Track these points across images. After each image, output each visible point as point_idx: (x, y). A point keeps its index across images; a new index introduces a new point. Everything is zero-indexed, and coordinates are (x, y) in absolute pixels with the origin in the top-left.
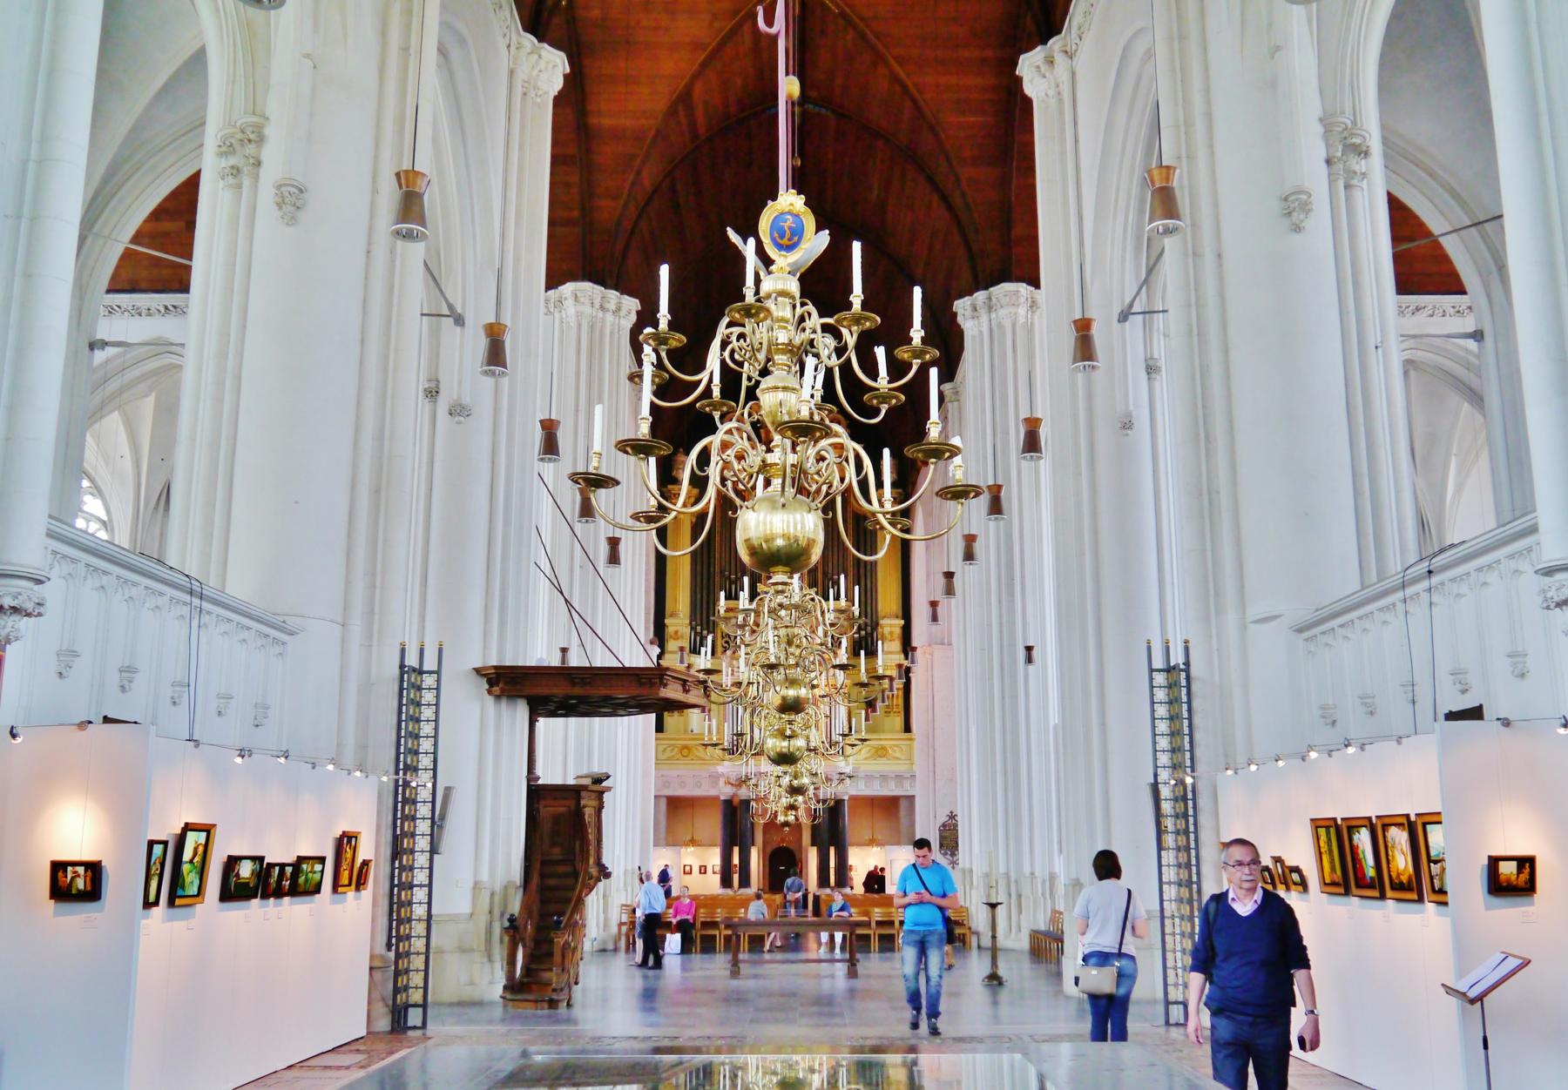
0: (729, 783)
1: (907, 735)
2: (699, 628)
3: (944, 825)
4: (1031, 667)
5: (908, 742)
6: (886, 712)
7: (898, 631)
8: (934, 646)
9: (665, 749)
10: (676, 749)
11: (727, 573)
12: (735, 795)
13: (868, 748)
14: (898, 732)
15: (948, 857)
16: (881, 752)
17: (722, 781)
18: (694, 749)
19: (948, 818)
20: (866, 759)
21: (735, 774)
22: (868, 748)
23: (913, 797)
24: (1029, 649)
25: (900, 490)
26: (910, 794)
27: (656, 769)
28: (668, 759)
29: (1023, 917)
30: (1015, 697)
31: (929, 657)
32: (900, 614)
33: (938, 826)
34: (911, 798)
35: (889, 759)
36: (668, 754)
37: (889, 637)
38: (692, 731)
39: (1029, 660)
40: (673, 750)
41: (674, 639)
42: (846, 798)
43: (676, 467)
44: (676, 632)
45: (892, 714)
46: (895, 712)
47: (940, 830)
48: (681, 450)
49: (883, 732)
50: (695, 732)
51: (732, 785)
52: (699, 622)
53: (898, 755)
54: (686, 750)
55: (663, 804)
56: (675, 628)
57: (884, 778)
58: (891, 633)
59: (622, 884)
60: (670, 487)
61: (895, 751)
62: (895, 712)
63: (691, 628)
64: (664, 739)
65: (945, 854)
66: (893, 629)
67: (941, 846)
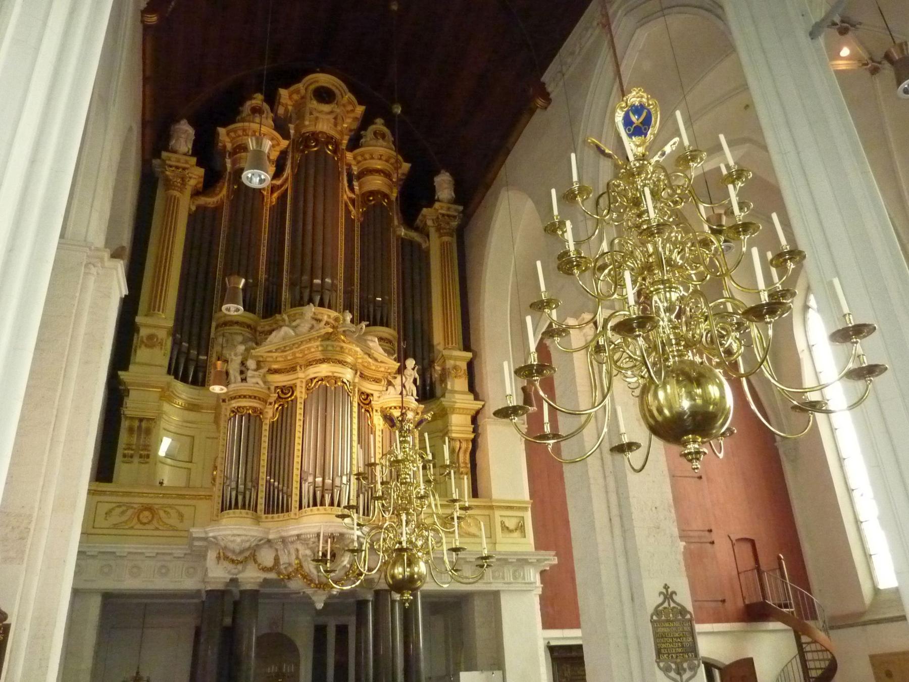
0: (226, 558)
3: (657, 612)
5: (486, 512)
7: (464, 365)
9: (113, 509)
10: (130, 512)
12: (234, 581)
15: (673, 674)
17: (211, 555)
18: (162, 513)
19: (662, 597)
21: (238, 540)
23: (496, 595)
25: (461, 208)
26: (493, 587)
27: (91, 492)
28: (115, 526)
36: (114, 519)
38: (161, 483)
40: (123, 513)
41: (146, 346)
44: (151, 337)
47: (652, 622)
50: (166, 483)
51: (233, 561)
54: (146, 513)
55: (95, 605)
60: (164, 154)
61: (469, 525)
64: (112, 493)
65: (666, 670)
66: (458, 363)
67: (659, 652)
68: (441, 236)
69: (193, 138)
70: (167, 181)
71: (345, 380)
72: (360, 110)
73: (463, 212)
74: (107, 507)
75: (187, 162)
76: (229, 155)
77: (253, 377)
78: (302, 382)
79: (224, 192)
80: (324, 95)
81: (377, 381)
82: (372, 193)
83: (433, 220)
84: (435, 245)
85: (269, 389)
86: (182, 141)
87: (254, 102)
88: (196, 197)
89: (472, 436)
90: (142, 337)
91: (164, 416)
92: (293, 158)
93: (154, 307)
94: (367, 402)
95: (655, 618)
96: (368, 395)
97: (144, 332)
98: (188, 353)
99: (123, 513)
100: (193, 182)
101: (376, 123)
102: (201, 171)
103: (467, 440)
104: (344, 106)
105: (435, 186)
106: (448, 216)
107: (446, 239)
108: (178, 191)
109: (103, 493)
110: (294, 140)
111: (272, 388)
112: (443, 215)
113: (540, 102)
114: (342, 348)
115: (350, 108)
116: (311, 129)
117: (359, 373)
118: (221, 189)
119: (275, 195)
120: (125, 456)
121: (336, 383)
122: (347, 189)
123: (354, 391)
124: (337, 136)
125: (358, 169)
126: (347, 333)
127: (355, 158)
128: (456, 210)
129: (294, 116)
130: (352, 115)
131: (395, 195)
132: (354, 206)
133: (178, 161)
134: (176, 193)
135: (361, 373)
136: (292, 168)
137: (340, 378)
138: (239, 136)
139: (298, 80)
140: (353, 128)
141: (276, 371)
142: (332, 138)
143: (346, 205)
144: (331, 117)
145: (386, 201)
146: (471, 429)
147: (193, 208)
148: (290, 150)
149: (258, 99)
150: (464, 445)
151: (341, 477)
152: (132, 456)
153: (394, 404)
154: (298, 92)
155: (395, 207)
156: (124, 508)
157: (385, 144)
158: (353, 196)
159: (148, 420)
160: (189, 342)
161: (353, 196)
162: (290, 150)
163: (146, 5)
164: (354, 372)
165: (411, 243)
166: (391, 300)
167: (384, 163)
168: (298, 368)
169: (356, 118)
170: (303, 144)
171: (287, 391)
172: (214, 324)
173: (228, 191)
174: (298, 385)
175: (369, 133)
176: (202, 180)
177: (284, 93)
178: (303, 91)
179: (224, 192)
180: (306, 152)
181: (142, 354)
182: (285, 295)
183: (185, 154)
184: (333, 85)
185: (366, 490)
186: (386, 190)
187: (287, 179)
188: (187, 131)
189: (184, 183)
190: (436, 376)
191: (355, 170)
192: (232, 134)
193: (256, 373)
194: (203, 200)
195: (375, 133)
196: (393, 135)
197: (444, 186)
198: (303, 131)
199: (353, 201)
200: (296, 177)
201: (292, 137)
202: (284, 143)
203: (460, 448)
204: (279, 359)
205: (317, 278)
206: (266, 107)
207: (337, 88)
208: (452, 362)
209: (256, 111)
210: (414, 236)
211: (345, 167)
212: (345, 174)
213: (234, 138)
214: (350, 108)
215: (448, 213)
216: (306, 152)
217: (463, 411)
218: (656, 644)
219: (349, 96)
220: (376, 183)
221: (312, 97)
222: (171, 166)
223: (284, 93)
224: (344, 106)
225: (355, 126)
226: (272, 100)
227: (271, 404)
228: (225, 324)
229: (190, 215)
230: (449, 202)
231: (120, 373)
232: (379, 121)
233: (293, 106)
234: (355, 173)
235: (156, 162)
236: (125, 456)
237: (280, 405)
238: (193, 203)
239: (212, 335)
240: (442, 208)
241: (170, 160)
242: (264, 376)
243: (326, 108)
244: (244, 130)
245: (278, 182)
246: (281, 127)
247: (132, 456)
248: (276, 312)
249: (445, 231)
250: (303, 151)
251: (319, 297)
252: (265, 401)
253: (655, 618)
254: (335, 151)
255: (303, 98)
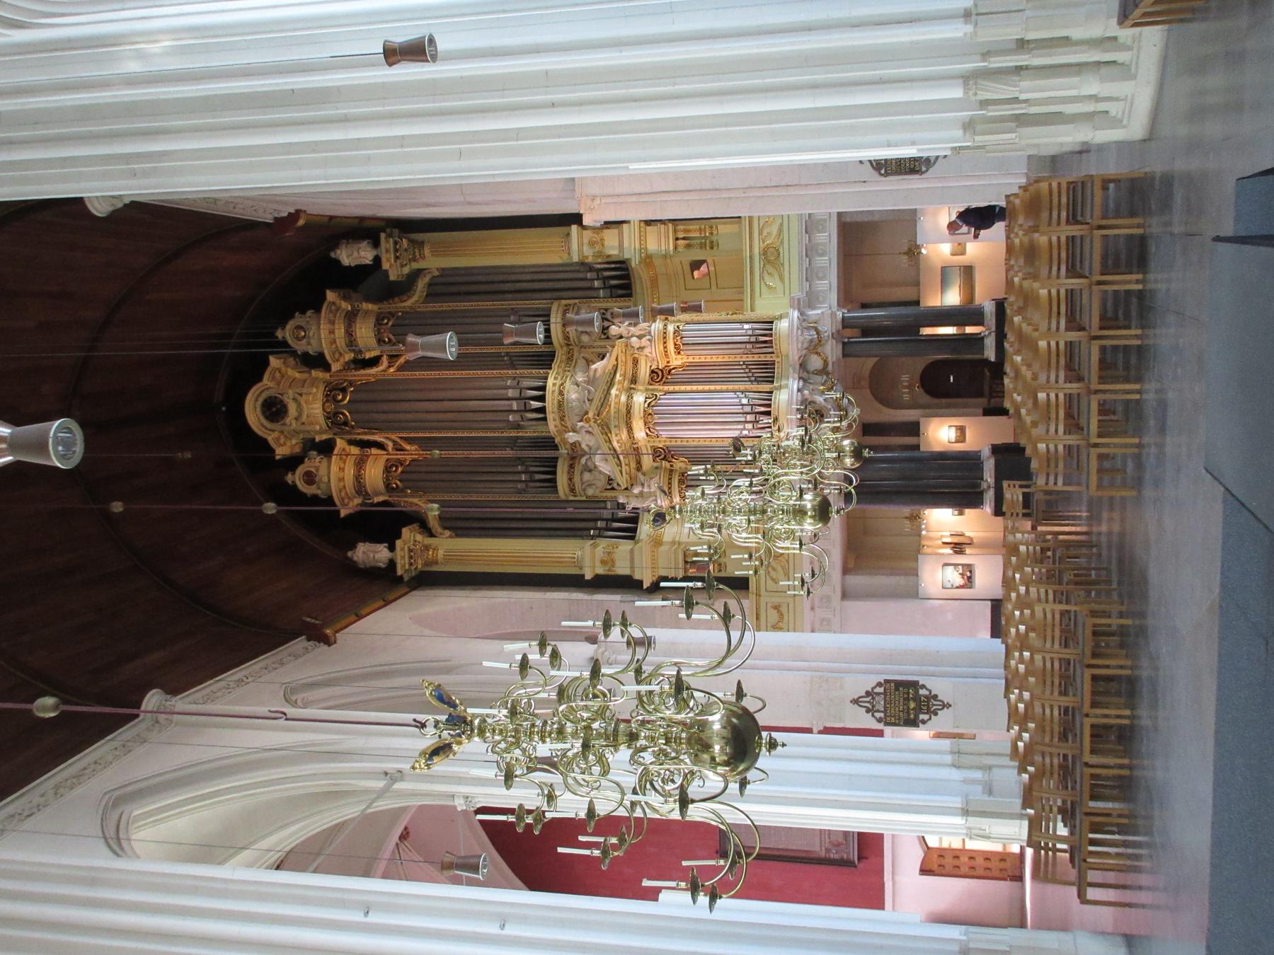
1: (743, 219)
2: (599, 524)
4: (442, 45)
6: (712, 248)
8: (578, 194)
9: (773, 580)
11: (519, 486)
13: (767, 277)
14: (740, 227)
16: (771, 257)
20: (782, 279)
22: (767, 277)
24: (393, 54)
25: (383, 235)
29: (1076, 33)
30: (548, 79)
31: (597, 201)
32: (563, 230)
33: (883, 179)
34: (839, 214)
35: (782, 242)
37: (597, 248)
39: (417, 51)
40: (774, 569)
42: (840, 314)
43: (373, 564)
44: (603, 562)
45: (714, 238)
46: (712, 234)
47: (886, 174)
48: (350, 554)
49: (742, 250)
52: (591, 524)
53: (774, 230)
55: (855, 580)
56: (598, 564)
57: (810, 251)
58: (592, 244)
59: (978, 775)
60: (399, 572)
62: (712, 234)
63: (600, 536)
64: (758, 582)
66: (586, 241)
68: (423, 258)
69: (367, 544)
70: (427, 564)
71: (646, 405)
72: (274, 361)
73: (384, 232)
74: (770, 582)
75: (402, 549)
76: (369, 499)
77: (649, 486)
78: (649, 441)
79: (415, 500)
80: (274, 409)
81: (636, 362)
82: (380, 341)
83: (402, 266)
84: (433, 262)
85: (657, 468)
86: (377, 556)
87: (298, 483)
88: (434, 531)
89: (670, 225)
90: (604, 570)
91: (677, 539)
92: (359, 434)
93: (571, 562)
94: (660, 373)
95: (883, 172)
96: (653, 372)
97: (600, 570)
98: (607, 520)
99: (774, 569)
100: (419, 537)
101: (283, 337)
102: (405, 531)
103: (675, 231)
104: (278, 383)
105: (357, 266)
106: (396, 250)
107: (427, 251)
108: (437, 556)
109: (758, 588)
110: (334, 434)
111: (656, 465)
112: (397, 258)
113: (301, 222)
114: (615, 412)
115: (278, 375)
116: (321, 420)
117: (633, 386)
118: (412, 503)
119: (408, 447)
120: (720, 571)
121: (650, 414)
122: (381, 368)
123: (652, 390)
124: (322, 388)
125: (347, 353)
126: (590, 398)
127: (338, 360)
128: (387, 242)
129: (301, 436)
130: (283, 369)
131: (370, 306)
132: (398, 356)
133: (403, 557)
134: (441, 552)
135: (631, 383)
136: (373, 434)
137: (645, 411)
138: (347, 494)
139: (265, 441)
140: (294, 362)
141: (639, 463)
142: (327, 395)
143: (400, 369)
144: (302, 400)
145: (386, 321)
146: (662, 226)
147: (448, 533)
148: (349, 437)
149: (296, 478)
150: (681, 235)
151: (743, 405)
152: (720, 565)
153: (662, 347)
154: (278, 439)
155: (387, 307)
156: (770, 569)
157: (314, 328)
158: (385, 360)
159: (685, 556)
160: (596, 520)
161: (385, 360)
162: (349, 437)
163: (322, 644)
164: (632, 391)
165: (430, 285)
166: (512, 309)
167: (337, 326)
168: (636, 446)
169: (284, 363)
170: (343, 427)
171: (659, 454)
172: (571, 498)
173: (414, 497)
174: (652, 444)
175: (300, 347)
176: (410, 527)
177: (281, 452)
178: (276, 434)
179: (415, 500)
180: (353, 423)
181: (622, 569)
182: (529, 433)
183: (392, 548)
184: (256, 400)
185: (750, 372)
186: (371, 322)
187: (387, 438)
188: (364, 553)
189: (427, 548)
190: (600, 260)
191: (349, 356)
192: (346, 501)
193: (646, 485)
194: (434, 523)
195: (299, 339)
196: (292, 317)
197: (353, 255)
198: (324, 426)
199: (393, 358)
200: (380, 430)
201: (331, 436)
202: (340, 444)
203: (684, 238)
204: (627, 462)
205: (511, 405)
206: (301, 470)
207: (259, 395)
208: (585, 248)
209: (310, 478)
210: (421, 284)
211: (354, 373)
212: (362, 372)
213: (349, 498)
214: (278, 375)
215: (392, 251)
216: (353, 423)
217: (643, 238)
218: (906, 173)
219: (266, 380)
220: (365, 333)
221: (282, 422)
222: (411, 564)
223: (281, 452)
224: (278, 383)
225: (291, 361)
226: (293, 462)
227: (672, 466)
228: (572, 490)
229: (458, 536)
230: (376, 244)
231: (645, 587)
232: (279, 334)
233: (291, 439)
234: (353, 355)
235: (406, 579)
236: (720, 571)
237: (672, 457)
238: (441, 534)
239: (584, 498)
240: (388, 260)
241: (405, 566)
242: (644, 474)
243: (292, 409)
244: (341, 491)
245: (390, 445)
246: (326, 448)
247: (720, 565)
248: (554, 442)
249: (417, 254)
250: (352, 427)
251: (532, 402)
252: (671, 471)
253: (883, 172)
254: (344, 390)
255: (282, 432)
